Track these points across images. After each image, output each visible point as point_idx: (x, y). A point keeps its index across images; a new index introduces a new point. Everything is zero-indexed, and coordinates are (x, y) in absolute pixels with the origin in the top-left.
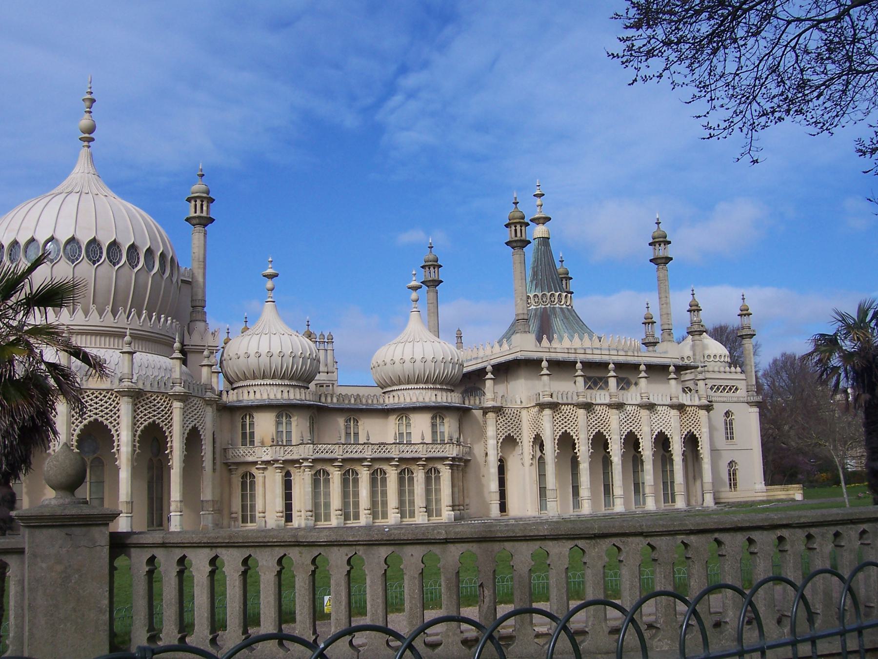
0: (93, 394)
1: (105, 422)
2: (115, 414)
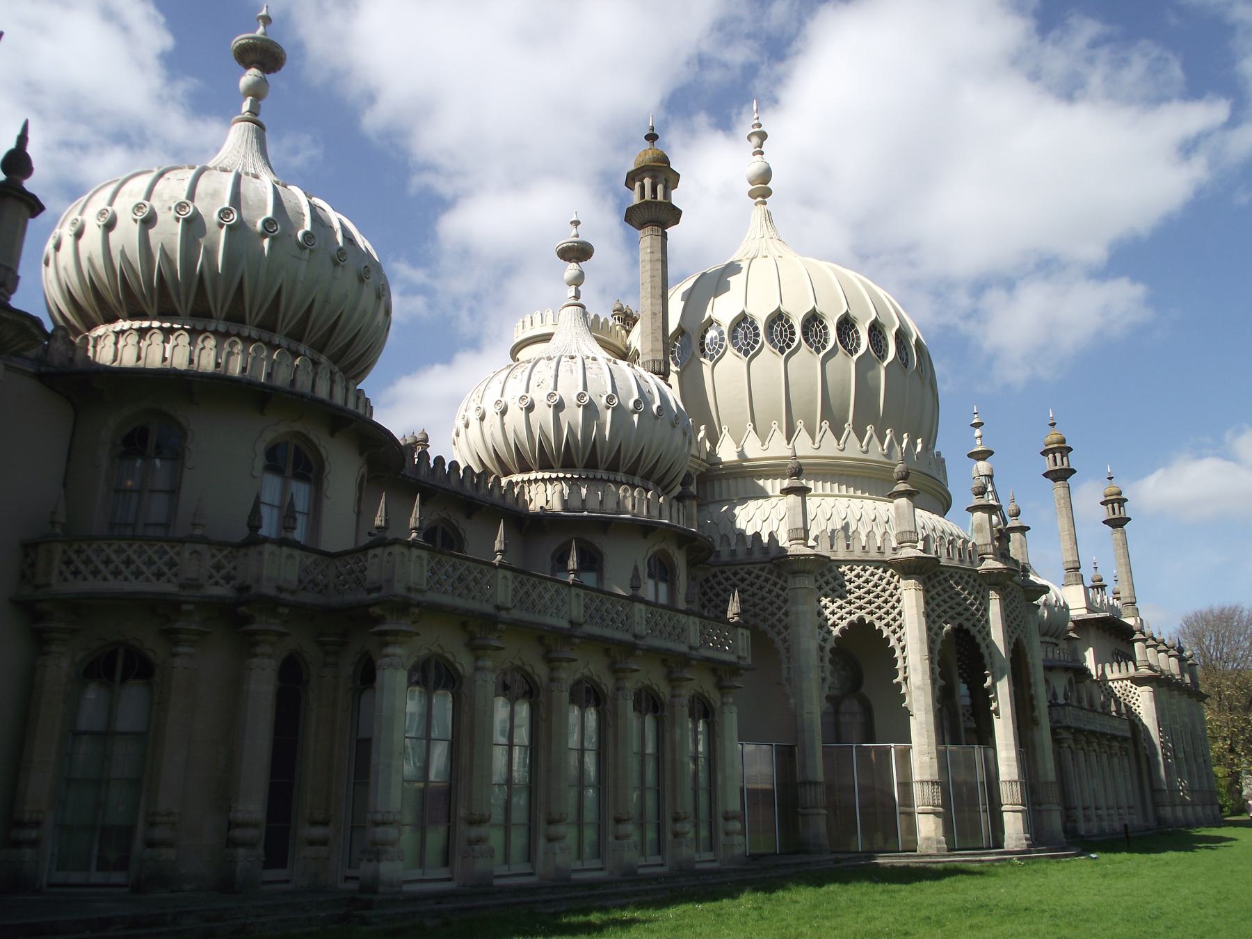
0: (851, 570)
1: (877, 625)
2: (893, 607)
